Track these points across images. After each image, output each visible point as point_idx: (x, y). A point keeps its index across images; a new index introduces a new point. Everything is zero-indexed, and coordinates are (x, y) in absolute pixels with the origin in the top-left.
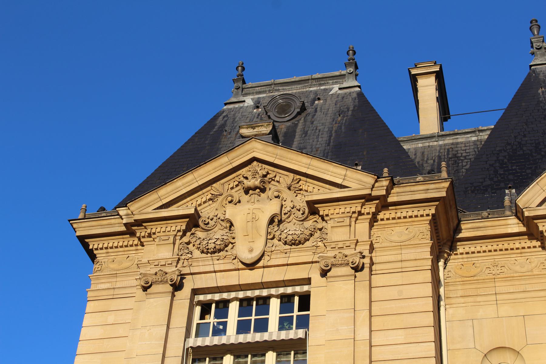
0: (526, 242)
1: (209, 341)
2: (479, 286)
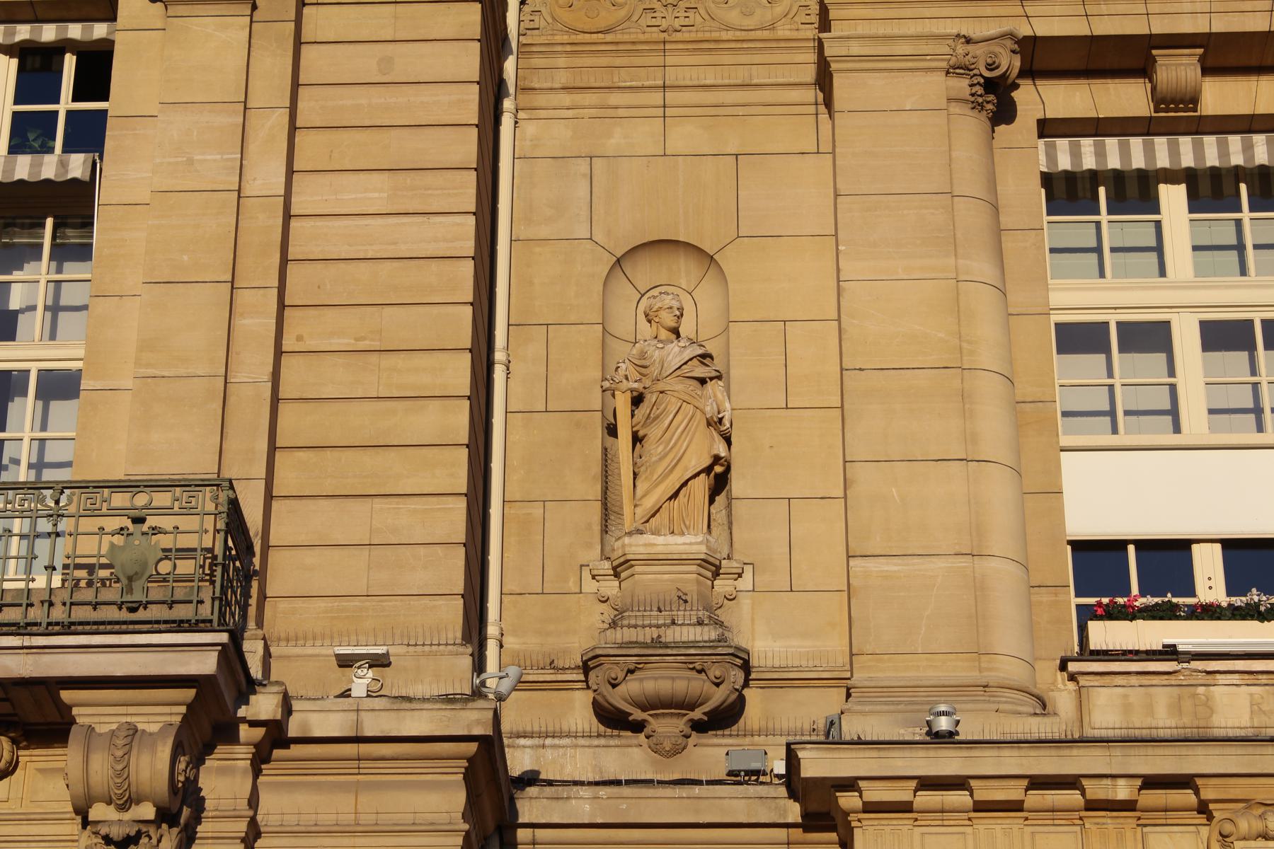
2: (618, 61)
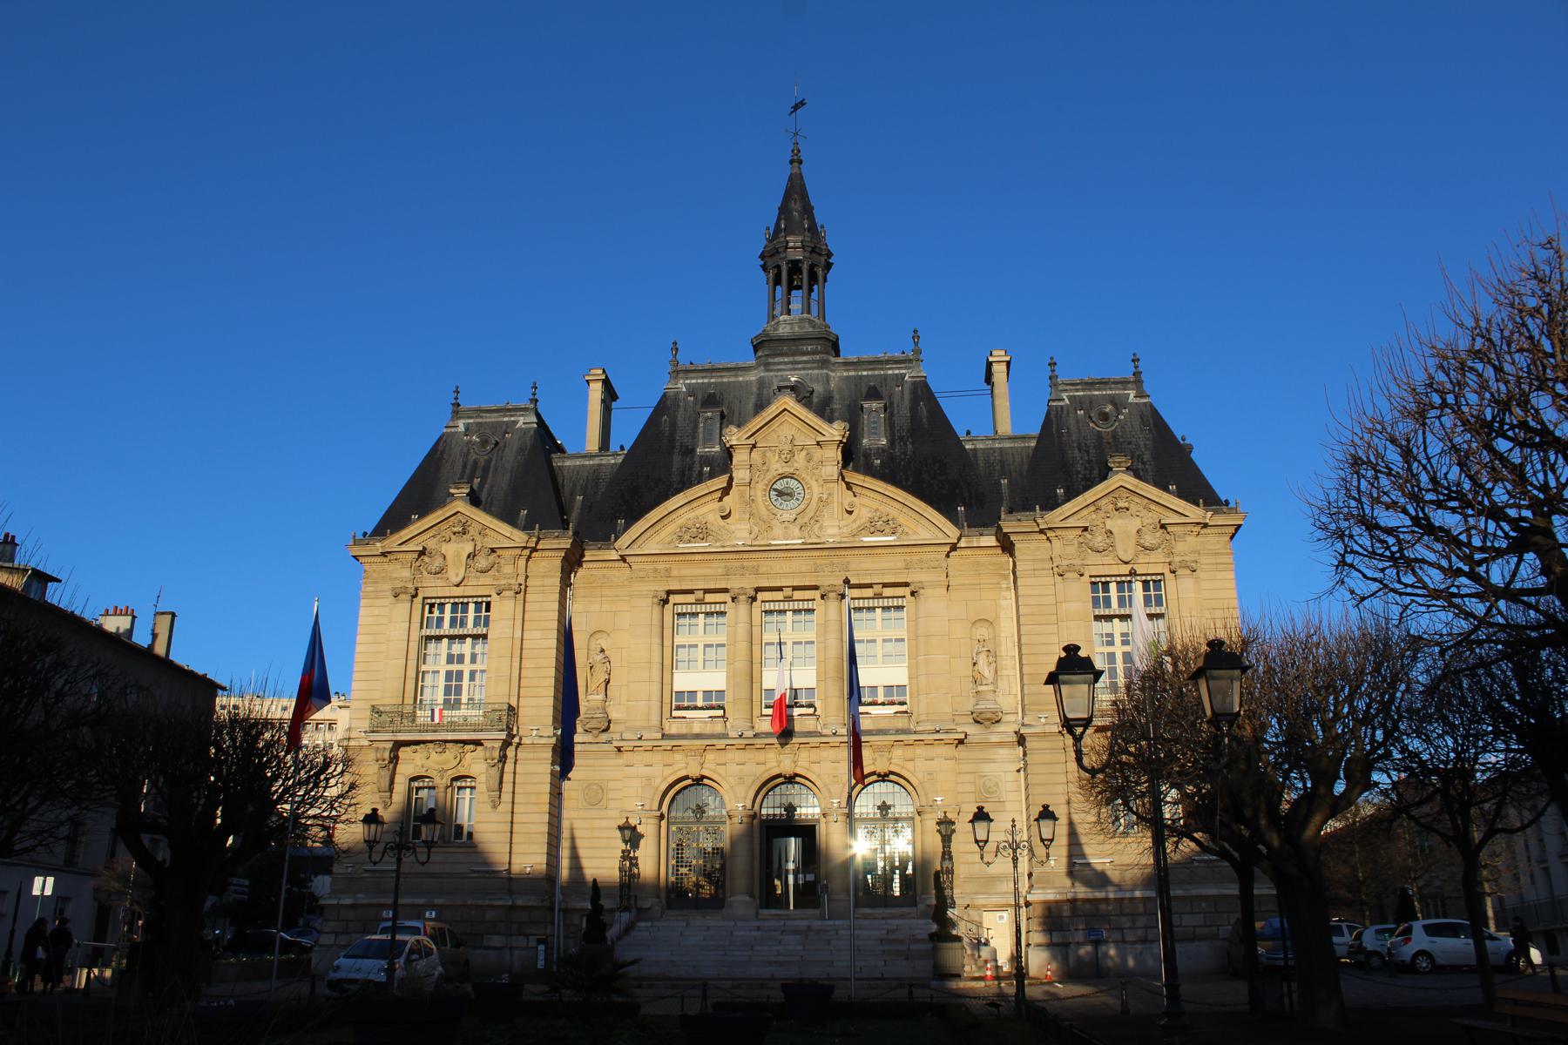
0: (621, 564)
1: (434, 632)
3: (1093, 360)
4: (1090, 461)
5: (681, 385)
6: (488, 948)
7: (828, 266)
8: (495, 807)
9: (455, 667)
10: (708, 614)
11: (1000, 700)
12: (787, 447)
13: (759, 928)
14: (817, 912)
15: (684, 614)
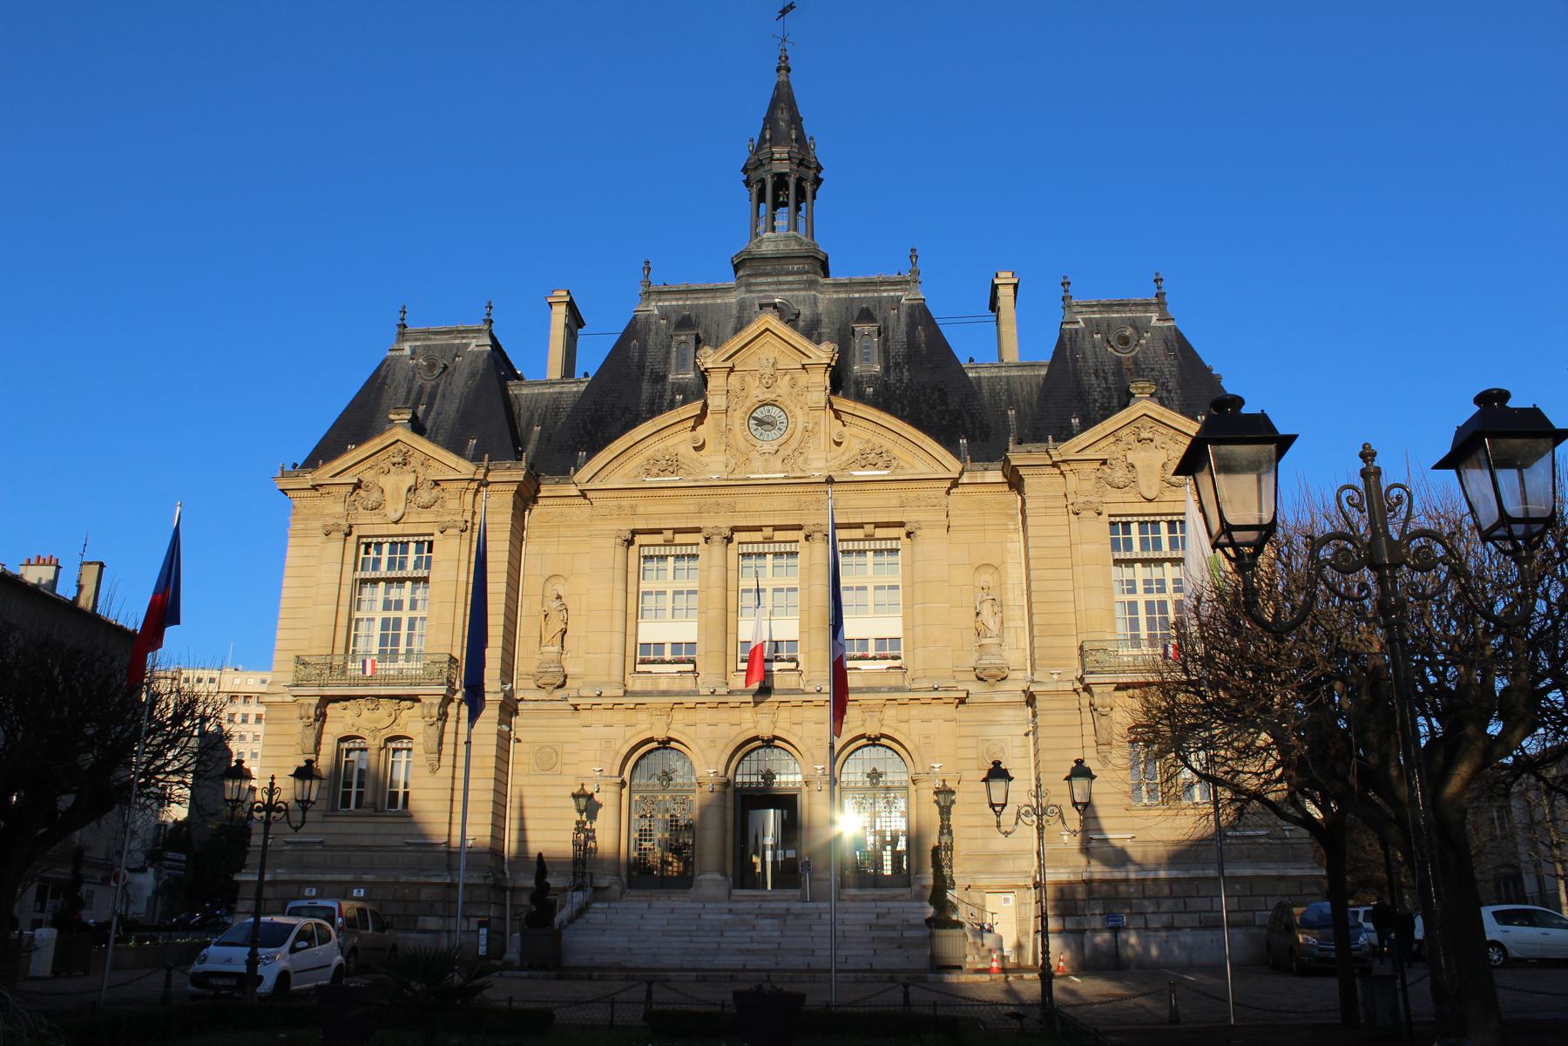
0: (582, 500)
1: (370, 574)
3: (1110, 278)
4: (1108, 389)
5: (654, 307)
6: (424, 931)
7: (818, 182)
8: (433, 771)
9: (392, 614)
10: (678, 557)
11: (1006, 654)
12: (769, 371)
13: (730, 911)
14: (797, 892)
15: (651, 557)
